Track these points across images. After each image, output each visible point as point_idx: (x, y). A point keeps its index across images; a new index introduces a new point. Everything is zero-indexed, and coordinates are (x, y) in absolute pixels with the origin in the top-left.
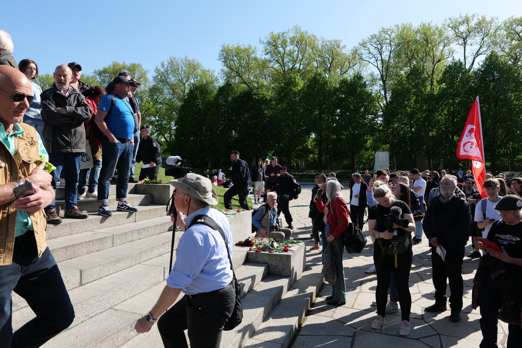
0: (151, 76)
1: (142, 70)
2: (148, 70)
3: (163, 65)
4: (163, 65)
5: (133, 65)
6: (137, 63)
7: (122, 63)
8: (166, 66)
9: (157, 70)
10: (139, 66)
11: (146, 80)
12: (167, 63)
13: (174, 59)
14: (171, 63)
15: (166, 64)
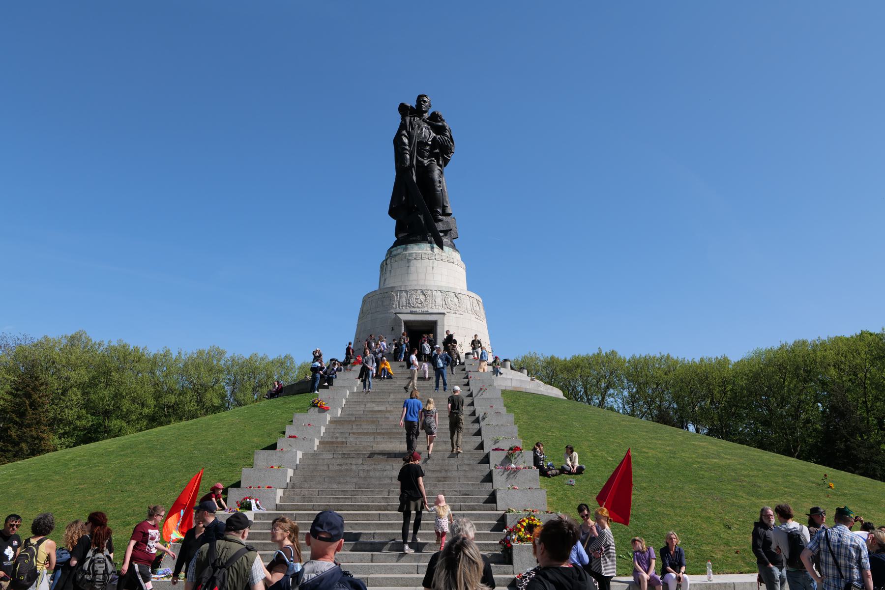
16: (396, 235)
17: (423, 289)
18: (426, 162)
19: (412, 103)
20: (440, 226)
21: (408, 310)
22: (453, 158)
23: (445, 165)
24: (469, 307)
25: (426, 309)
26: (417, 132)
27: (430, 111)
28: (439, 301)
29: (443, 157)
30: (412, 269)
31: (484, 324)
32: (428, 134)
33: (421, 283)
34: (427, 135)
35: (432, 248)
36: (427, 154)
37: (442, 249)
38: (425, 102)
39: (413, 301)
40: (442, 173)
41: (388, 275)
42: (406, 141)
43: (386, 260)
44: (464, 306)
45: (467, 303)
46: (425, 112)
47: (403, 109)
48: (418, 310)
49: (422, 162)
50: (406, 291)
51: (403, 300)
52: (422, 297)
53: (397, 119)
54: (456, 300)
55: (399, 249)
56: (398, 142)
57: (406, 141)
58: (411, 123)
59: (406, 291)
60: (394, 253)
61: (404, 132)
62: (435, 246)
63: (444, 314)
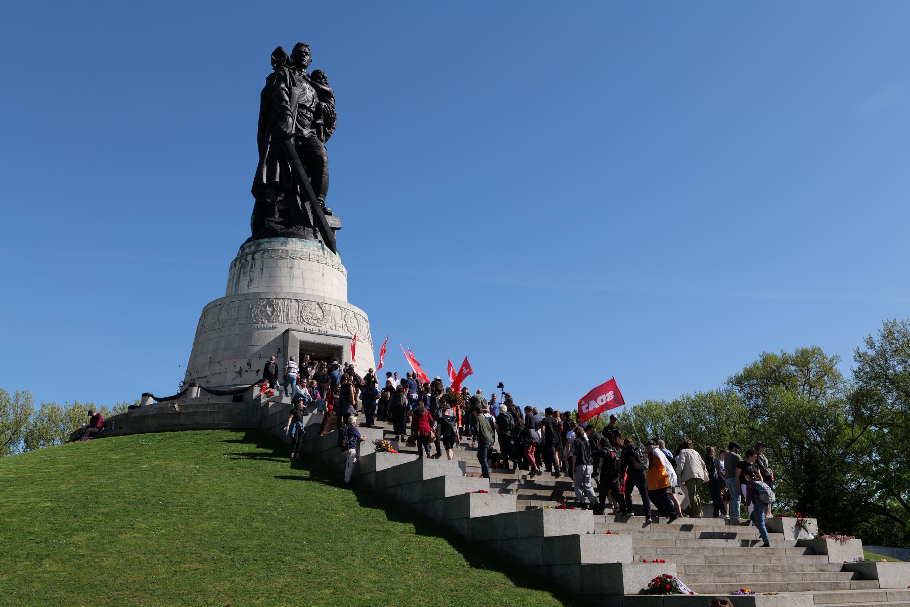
0: (847, 370)
1: (823, 358)
2: (837, 357)
3: (871, 345)
4: (871, 345)
5: (804, 353)
6: (809, 347)
7: (779, 355)
8: (877, 344)
9: (860, 356)
10: (816, 351)
11: (836, 377)
12: (879, 338)
13: (895, 324)
14: (889, 335)
15: (878, 341)
17: (320, 301)
18: (306, 132)
19: (288, 52)
20: (331, 221)
21: (301, 327)
22: (335, 135)
25: (323, 329)
26: (297, 91)
29: (324, 129)
30: (297, 272)
32: (307, 93)
33: (309, 292)
34: (311, 99)
35: (323, 248)
36: (307, 122)
38: (307, 54)
39: (306, 315)
41: (256, 274)
42: (287, 98)
46: (305, 67)
48: (316, 329)
49: (301, 132)
50: (296, 300)
51: (293, 313)
52: (319, 313)
55: (266, 243)
57: (287, 98)
58: (292, 78)
59: (296, 300)
61: (283, 86)
62: (325, 246)
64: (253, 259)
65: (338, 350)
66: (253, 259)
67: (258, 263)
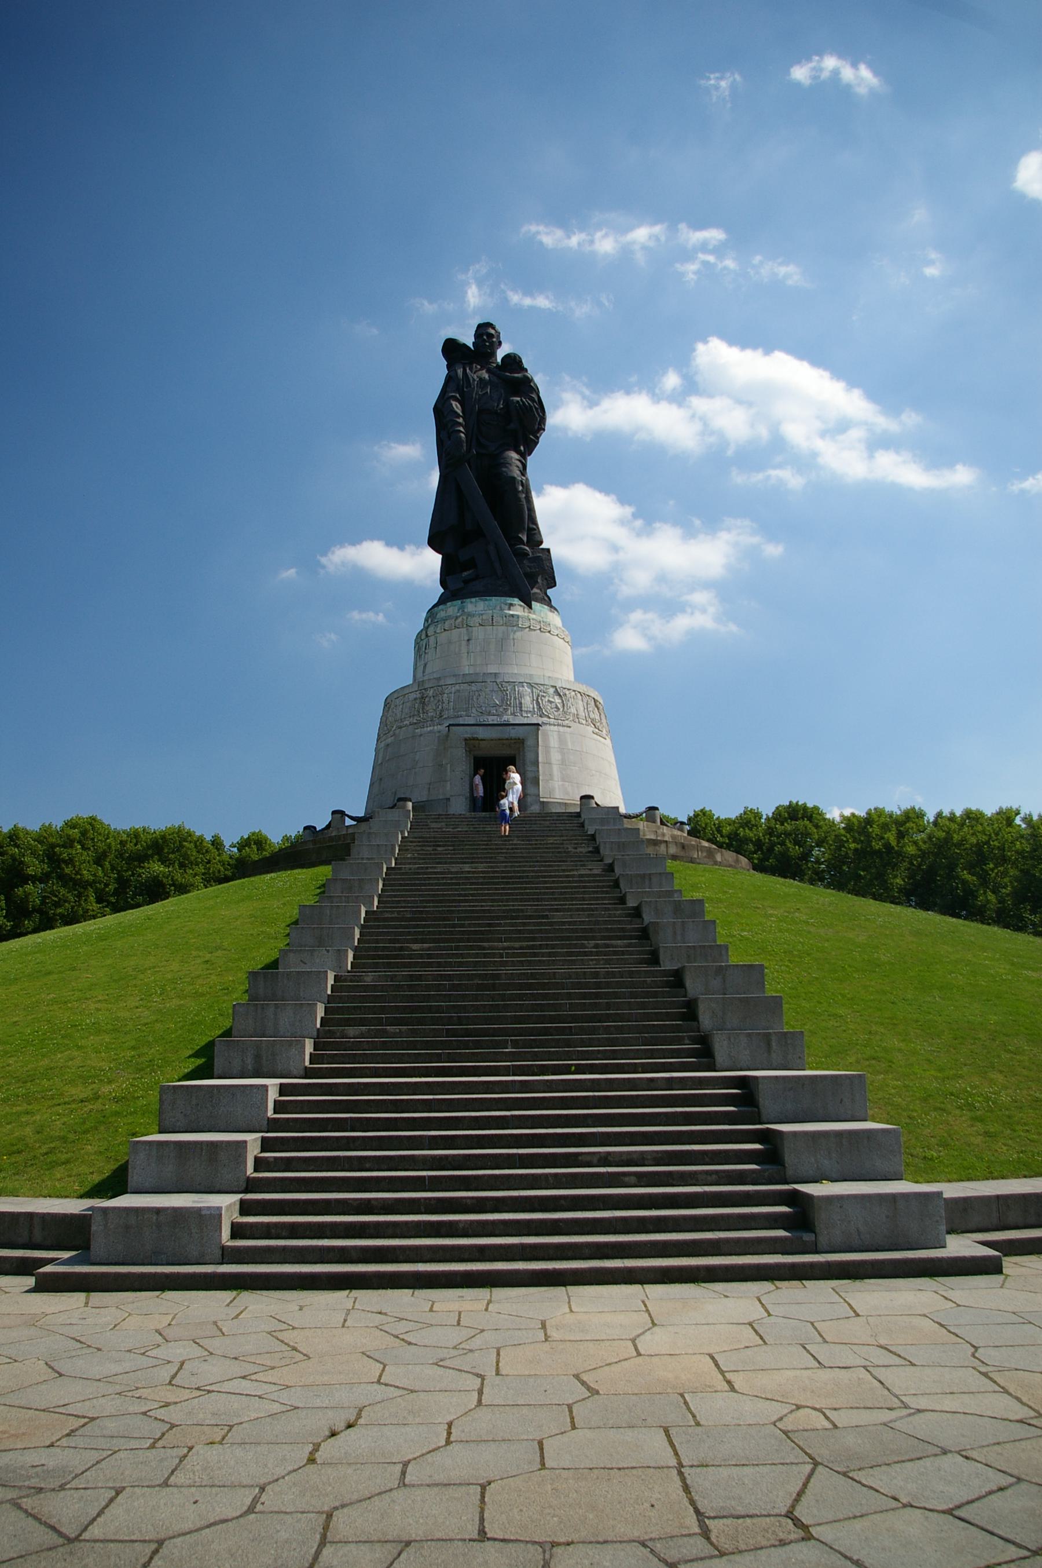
16: (443, 583)
19: (468, 339)
23: (530, 454)
24: (582, 714)
27: (500, 354)
28: (527, 702)
31: (608, 742)
37: (530, 607)
38: (491, 336)
40: (525, 467)
42: (456, 406)
43: (426, 628)
44: (573, 710)
45: (578, 706)
47: (452, 349)
48: (491, 720)
53: (440, 369)
54: (557, 700)
56: (441, 411)
57: (456, 406)
60: (442, 614)
63: (538, 725)
64: (427, 636)
65: (520, 742)
66: (427, 636)
67: (432, 639)
